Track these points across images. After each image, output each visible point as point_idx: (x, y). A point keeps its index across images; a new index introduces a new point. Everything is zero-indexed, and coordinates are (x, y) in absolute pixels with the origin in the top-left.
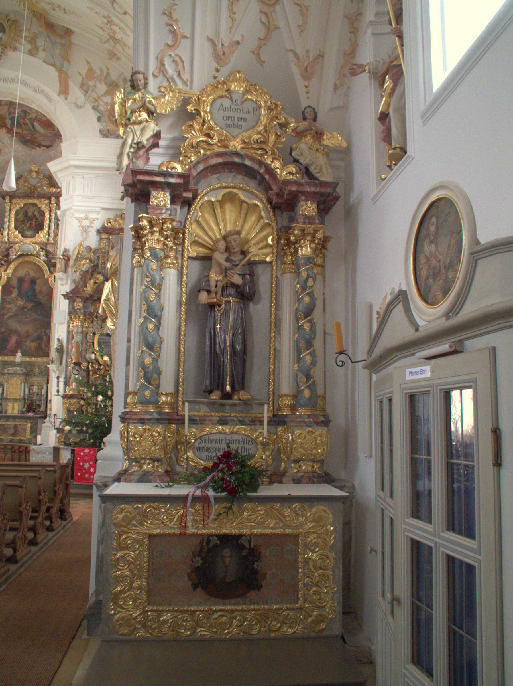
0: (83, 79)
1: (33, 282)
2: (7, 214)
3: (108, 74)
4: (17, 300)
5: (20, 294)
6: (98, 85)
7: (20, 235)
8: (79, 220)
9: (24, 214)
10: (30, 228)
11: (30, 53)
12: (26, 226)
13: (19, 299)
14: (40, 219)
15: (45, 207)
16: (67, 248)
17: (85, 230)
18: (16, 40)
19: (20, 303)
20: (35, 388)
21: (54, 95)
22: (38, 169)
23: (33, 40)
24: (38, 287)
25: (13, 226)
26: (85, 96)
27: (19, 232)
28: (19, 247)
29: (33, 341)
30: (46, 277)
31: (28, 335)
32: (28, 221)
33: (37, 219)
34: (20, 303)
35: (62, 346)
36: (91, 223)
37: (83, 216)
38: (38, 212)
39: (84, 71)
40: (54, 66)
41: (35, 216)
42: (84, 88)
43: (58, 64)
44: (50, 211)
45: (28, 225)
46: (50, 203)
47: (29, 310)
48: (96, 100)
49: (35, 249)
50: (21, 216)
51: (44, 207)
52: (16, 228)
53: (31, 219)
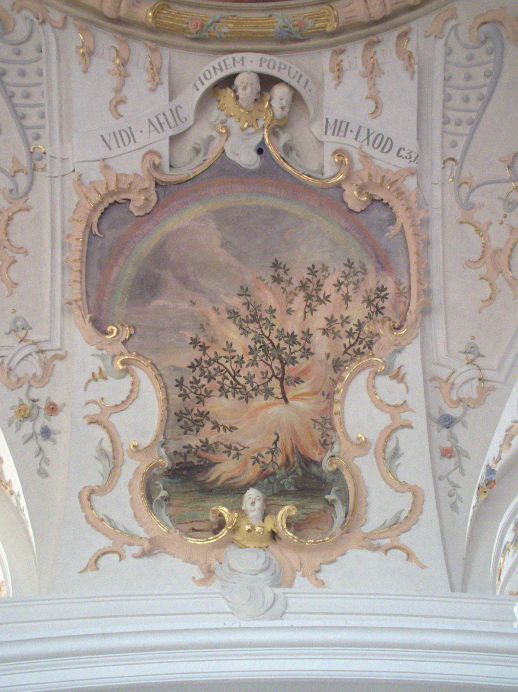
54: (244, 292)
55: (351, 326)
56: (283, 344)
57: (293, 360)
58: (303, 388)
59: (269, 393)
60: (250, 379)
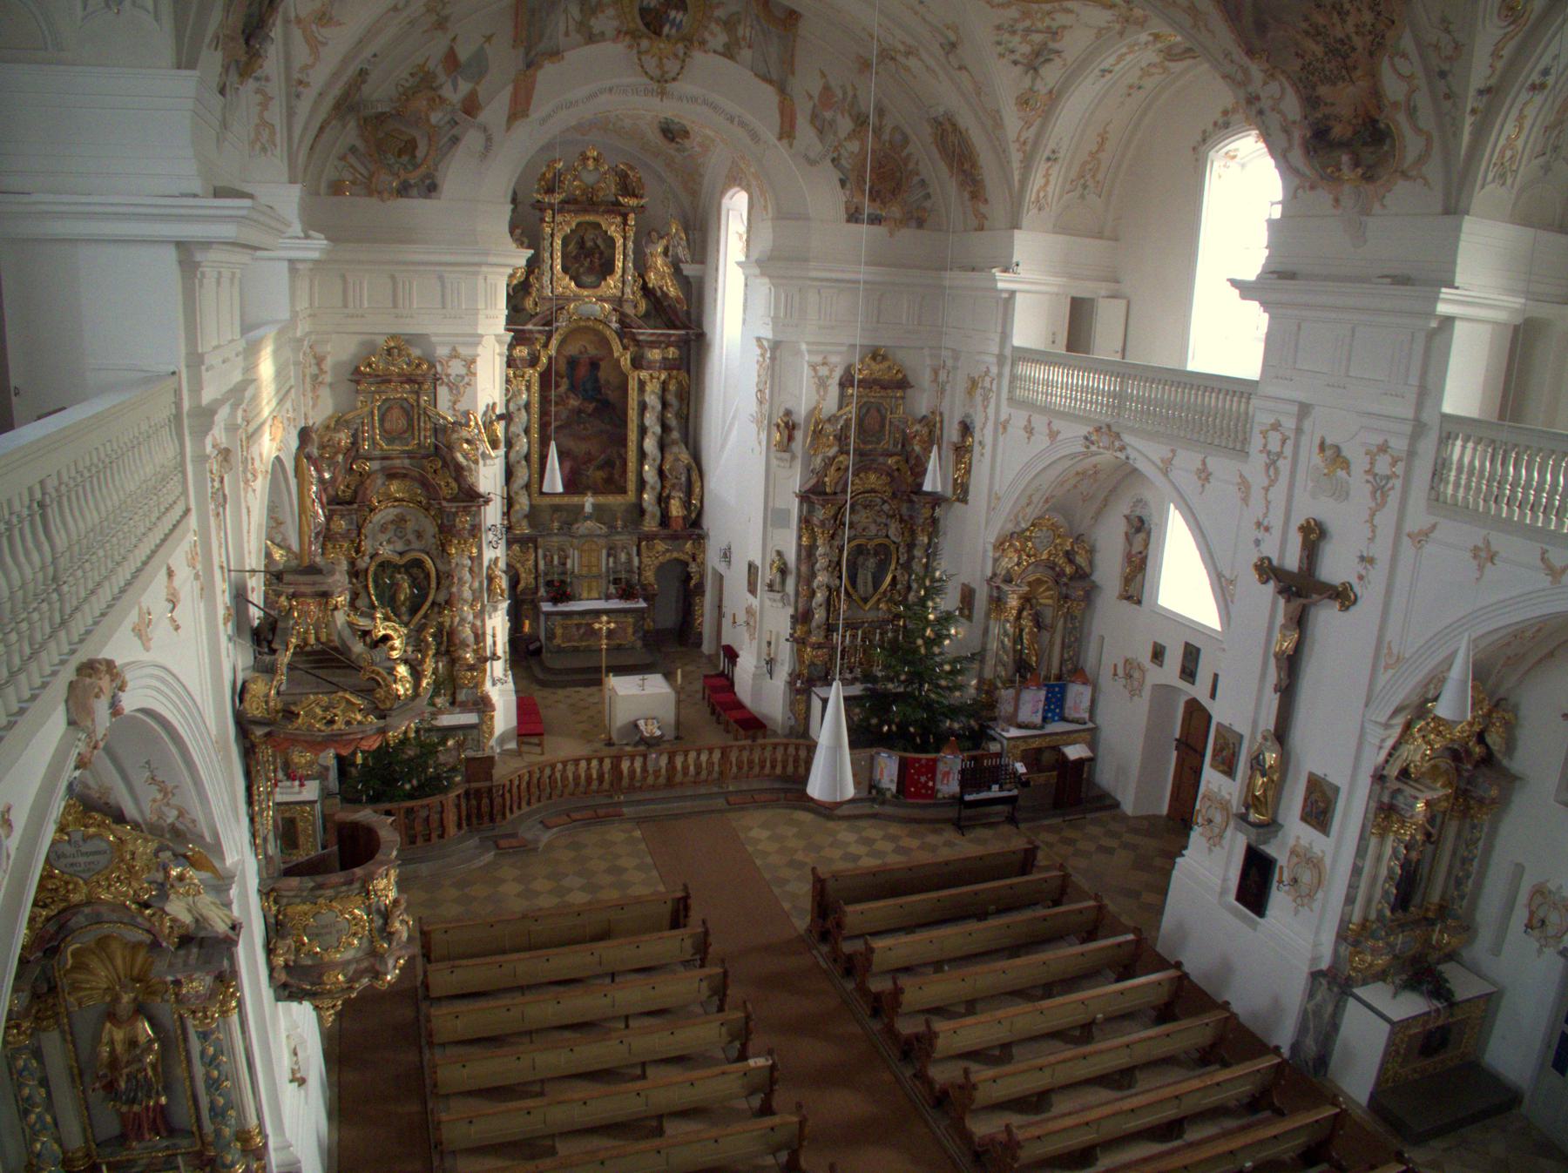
0: (815, 106)
1: (594, 365)
2: (547, 243)
3: (855, 96)
4: (568, 397)
5: (573, 388)
6: (839, 116)
7: (573, 284)
8: (814, 367)
9: (577, 243)
10: (591, 270)
11: (729, 52)
12: (582, 265)
13: (572, 395)
14: (607, 253)
15: (616, 231)
16: (789, 405)
17: (822, 383)
18: (706, 27)
19: (574, 402)
20: (623, 557)
21: (770, 136)
22: (599, 154)
23: (729, 25)
24: (602, 375)
25: (559, 267)
26: (821, 140)
27: (571, 278)
28: (576, 308)
29: (600, 468)
30: (616, 355)
31: (589, 458)
32: (586, 257)
33: (601, 253)
34: (574, 402)
35: (785, 564)
36: (831, 371)
37: (818, 359)
38: (604, 240)
39: (815, 87)
40: (769, 81)
41: (598, 247)
42: (822, 128)
43: (775, 77)
44: (625, 238)
45: (586, 264)
46: (625, 223)
47: (590, 415)
48: (836, 149)
49: (603, 308)
50: (571, 247)
51: (613, 231)
52: (565, 269)
53: (589, 254)
54: (1306, 19)
55: (1369, 27)
56: (1338, 46)
57: (1348, 56)
58: (1359, 73)
59: (1344, 80)
60: (1331, 71)
